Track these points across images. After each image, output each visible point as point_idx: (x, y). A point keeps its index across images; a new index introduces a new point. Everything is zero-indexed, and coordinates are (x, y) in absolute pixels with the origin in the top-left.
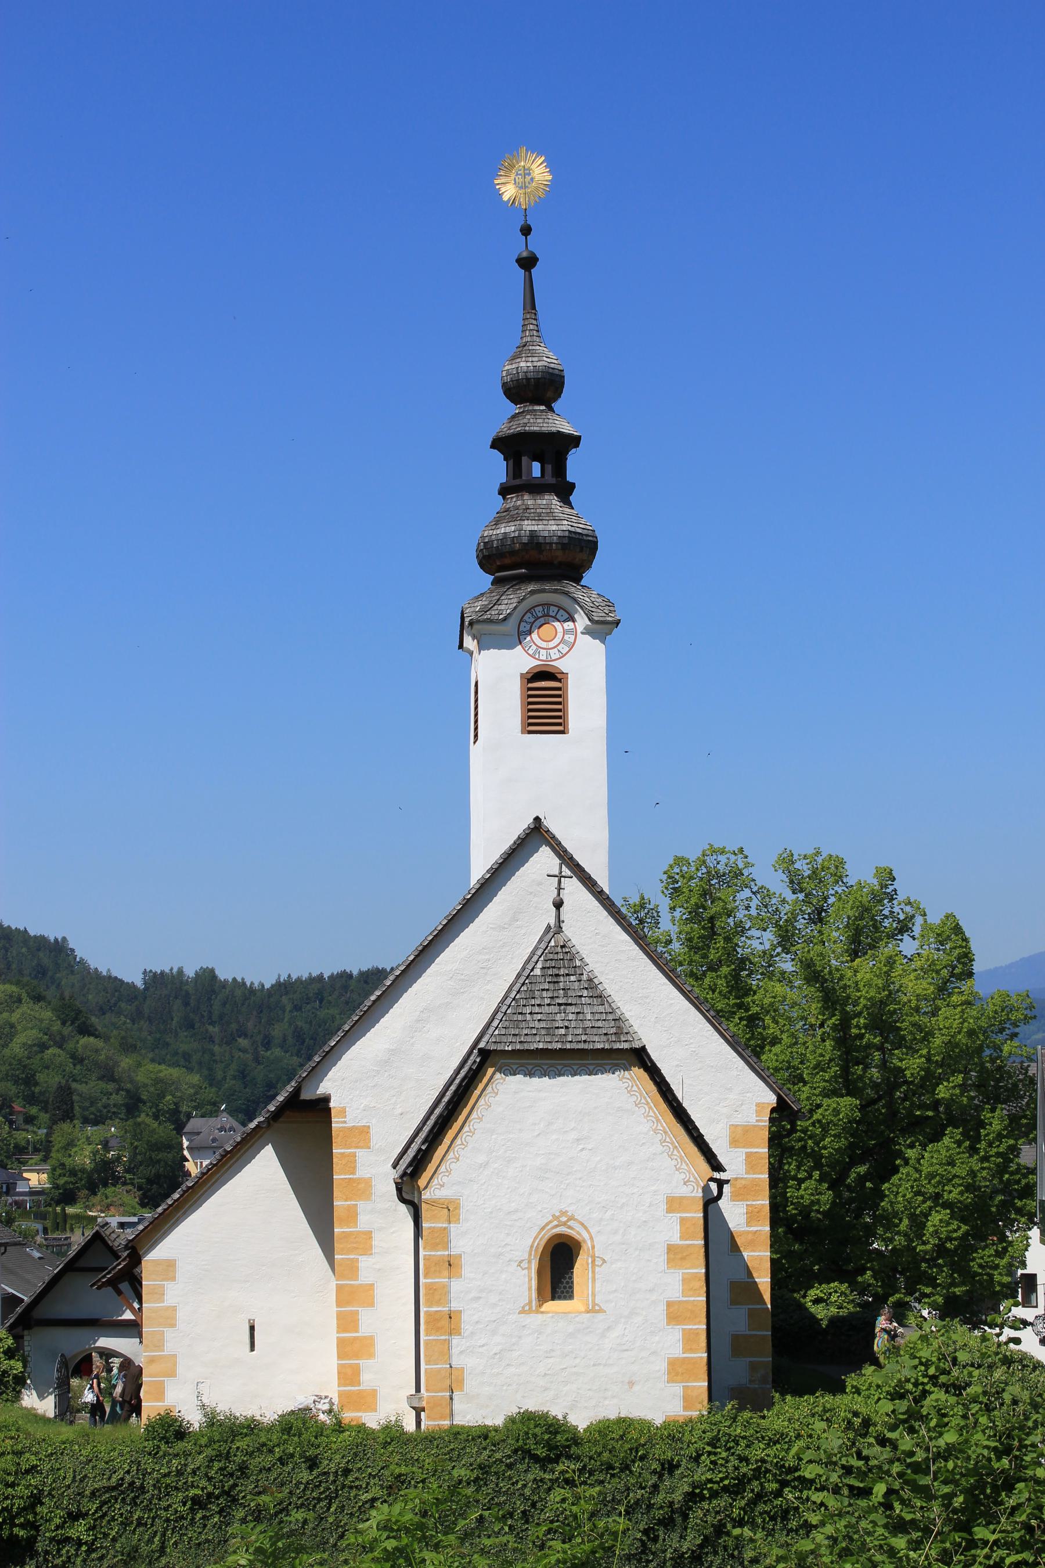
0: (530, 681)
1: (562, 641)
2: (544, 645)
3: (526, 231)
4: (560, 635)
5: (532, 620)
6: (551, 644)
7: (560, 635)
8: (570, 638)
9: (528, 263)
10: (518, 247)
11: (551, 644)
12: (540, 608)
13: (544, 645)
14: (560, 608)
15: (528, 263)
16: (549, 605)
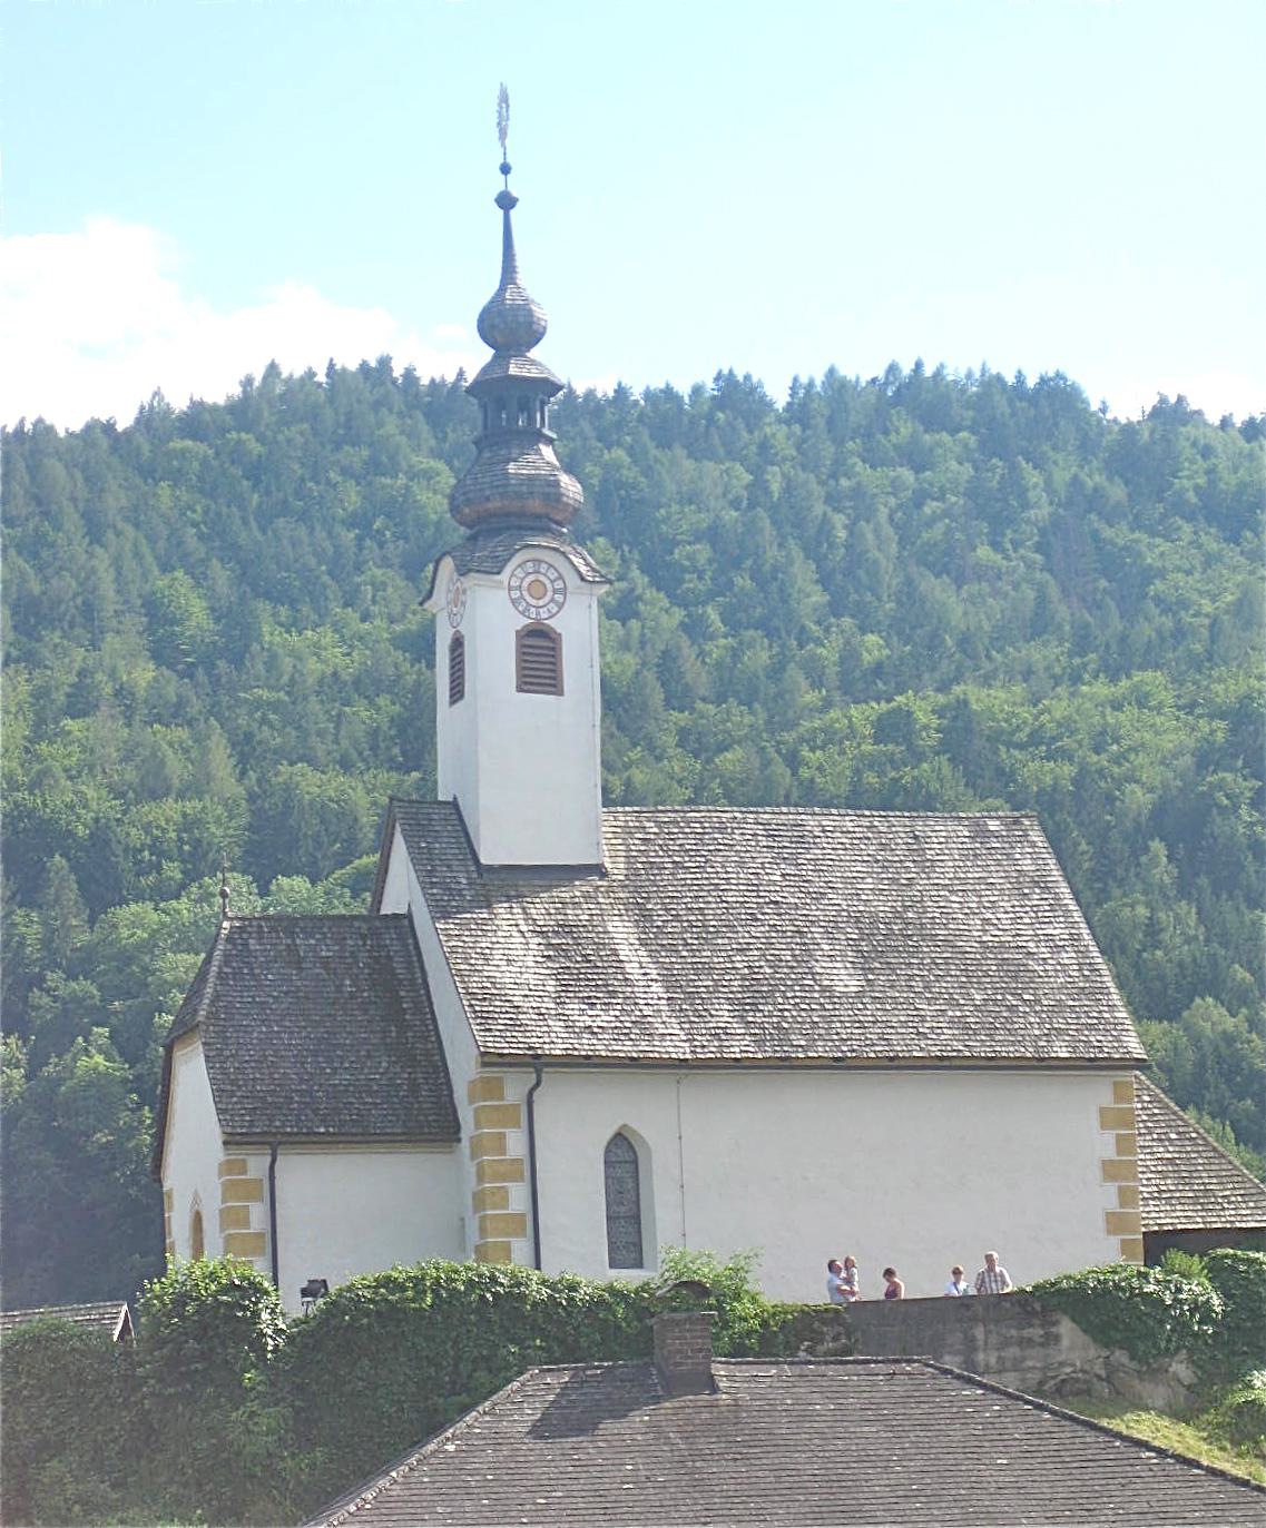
0: (523, 637)
1: (552, 600)
2: (533, 602)
3: (505, 169)
4: (550, 594)
5: (522, 575)
6: (541, 603)
7: (550, 594)
8: (559, 598)
9: (506, 202)
10: (497, 184)
11: (541, 603)
12: (530, 564)
13: (533, 602)
14: (551, 566)
15: (506, 202)
16: (540, 561)
